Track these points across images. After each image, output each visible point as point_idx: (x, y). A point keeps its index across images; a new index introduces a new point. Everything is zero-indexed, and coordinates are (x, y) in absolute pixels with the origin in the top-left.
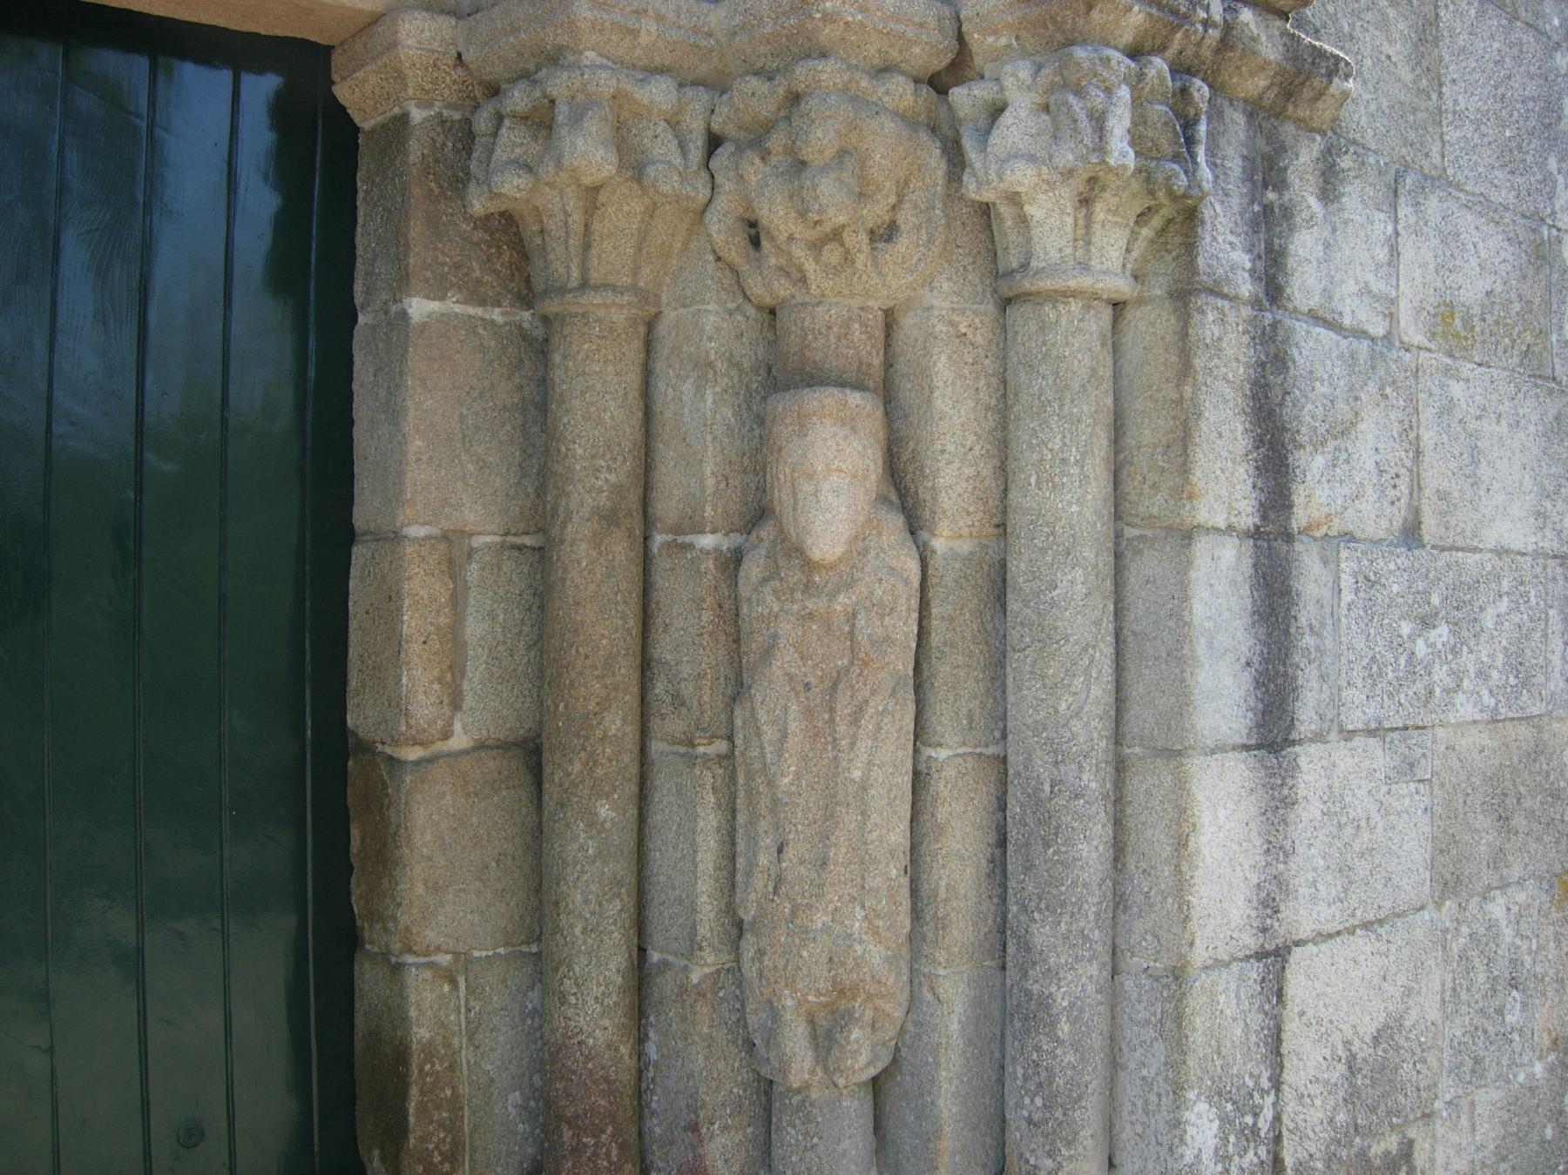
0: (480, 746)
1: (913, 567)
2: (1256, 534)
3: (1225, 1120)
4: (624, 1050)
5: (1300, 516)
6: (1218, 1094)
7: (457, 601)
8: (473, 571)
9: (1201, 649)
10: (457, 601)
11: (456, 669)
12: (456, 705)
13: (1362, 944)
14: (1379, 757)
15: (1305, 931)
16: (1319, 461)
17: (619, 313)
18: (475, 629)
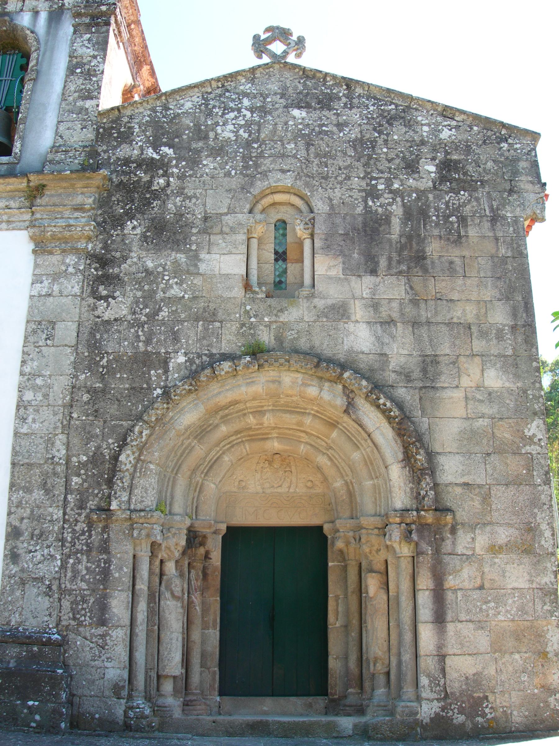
0: (341, 626)
1: (385, 598)
2: (434, 590)
3: (430, 681)
4: (356, 670)
5: (447, 585)
6: (428, 676)
7: (337, 605)
8: (340, 601)
9: (421, 607)
10: (337, 605)
11: (337, 615)
12: (337, 619)
13: (470, 658)
14: (471, 626)
15: (451, 652)
16: (451, 577)
17: (354, 563)
18: (340, 609)
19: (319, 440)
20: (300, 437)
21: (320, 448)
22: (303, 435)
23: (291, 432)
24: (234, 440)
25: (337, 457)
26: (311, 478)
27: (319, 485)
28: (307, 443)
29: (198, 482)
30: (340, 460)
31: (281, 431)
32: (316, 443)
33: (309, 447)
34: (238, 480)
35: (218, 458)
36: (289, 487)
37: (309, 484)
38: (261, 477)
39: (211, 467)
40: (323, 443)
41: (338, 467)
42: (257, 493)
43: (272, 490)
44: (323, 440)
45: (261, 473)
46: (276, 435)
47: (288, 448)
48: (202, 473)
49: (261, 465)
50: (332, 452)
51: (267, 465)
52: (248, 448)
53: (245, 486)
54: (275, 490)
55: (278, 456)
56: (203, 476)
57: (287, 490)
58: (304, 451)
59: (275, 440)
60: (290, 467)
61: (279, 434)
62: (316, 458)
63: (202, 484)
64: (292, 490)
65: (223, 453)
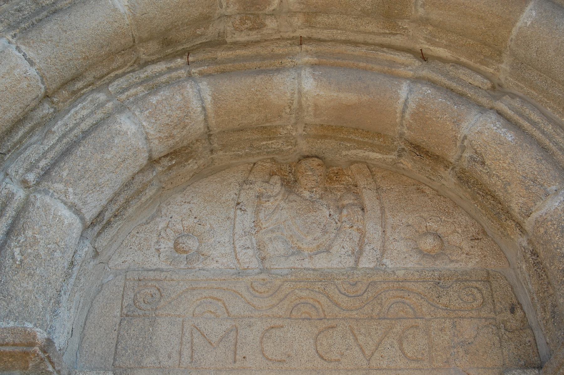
19: (461, 73)
20: (392, 63)
21: (470, 93)
22: (400, 58)
23: (360, 51)
24: (161, 74)
25: (535, 117)
26: (434, 226)
27: (466, 246)
28: (417, 80)
29: (10, 197)
30: (549, 128)
31: (324, 48)
32: (452, 79)
33: (428, 90)
34: (172, 235)
35: (95, 126)
36: (358, 254)
37: (428, 243)
38: (256, 223)
39: (66, 153)
40: (478, 80)
41: (544, 149)
42: (241, 273)
43: (293, 262)
44: (478, 72)
45: (257, 212)
46: (306, 59)
47: (350, 97)
48: (28, 170)
49: (258, 187)
50: (517, 104)
51: (278, 188)
52: (208, 99)
53: (198, 252)
54: (307, 264)
55: (317, 161)
56: (31, 177)
57: (350, 262)
58: (412, 105)
59: (306, 73)
60: (358, 196)
61: (317, 54)
62: (457, 122)
63: (26, 204)
64: (366, 263)
65: (121, 108)
